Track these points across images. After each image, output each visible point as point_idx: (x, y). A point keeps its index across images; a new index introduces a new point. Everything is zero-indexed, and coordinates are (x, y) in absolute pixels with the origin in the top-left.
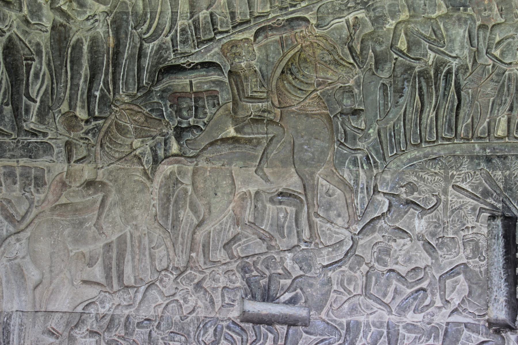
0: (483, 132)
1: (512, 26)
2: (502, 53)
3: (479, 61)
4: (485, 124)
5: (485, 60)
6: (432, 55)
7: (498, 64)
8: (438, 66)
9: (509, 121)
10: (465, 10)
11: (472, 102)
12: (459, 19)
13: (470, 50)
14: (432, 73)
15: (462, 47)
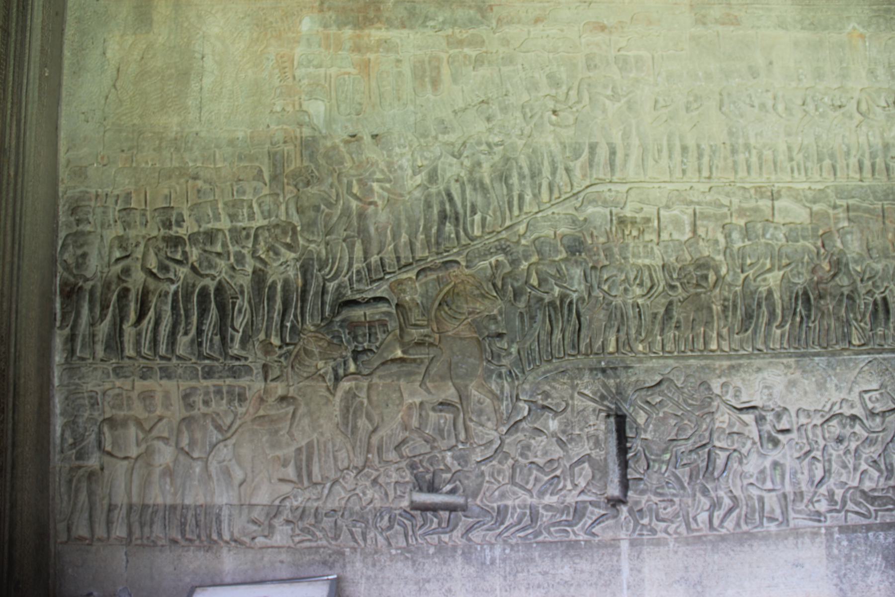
0: (598, 349)
1: (614, 267)
2: (609, 288)
3: (593, 294)
4: (600, 343)
5: (597, 293)
6: (557, 290)
7: (607, 296)
8: (563, 297)
9: (617, 340)
10: (580, 255)
11: (589, 325)
12: (576, 262)
13: (586, 286)
14: (558, 303)
15: (580, 284)
